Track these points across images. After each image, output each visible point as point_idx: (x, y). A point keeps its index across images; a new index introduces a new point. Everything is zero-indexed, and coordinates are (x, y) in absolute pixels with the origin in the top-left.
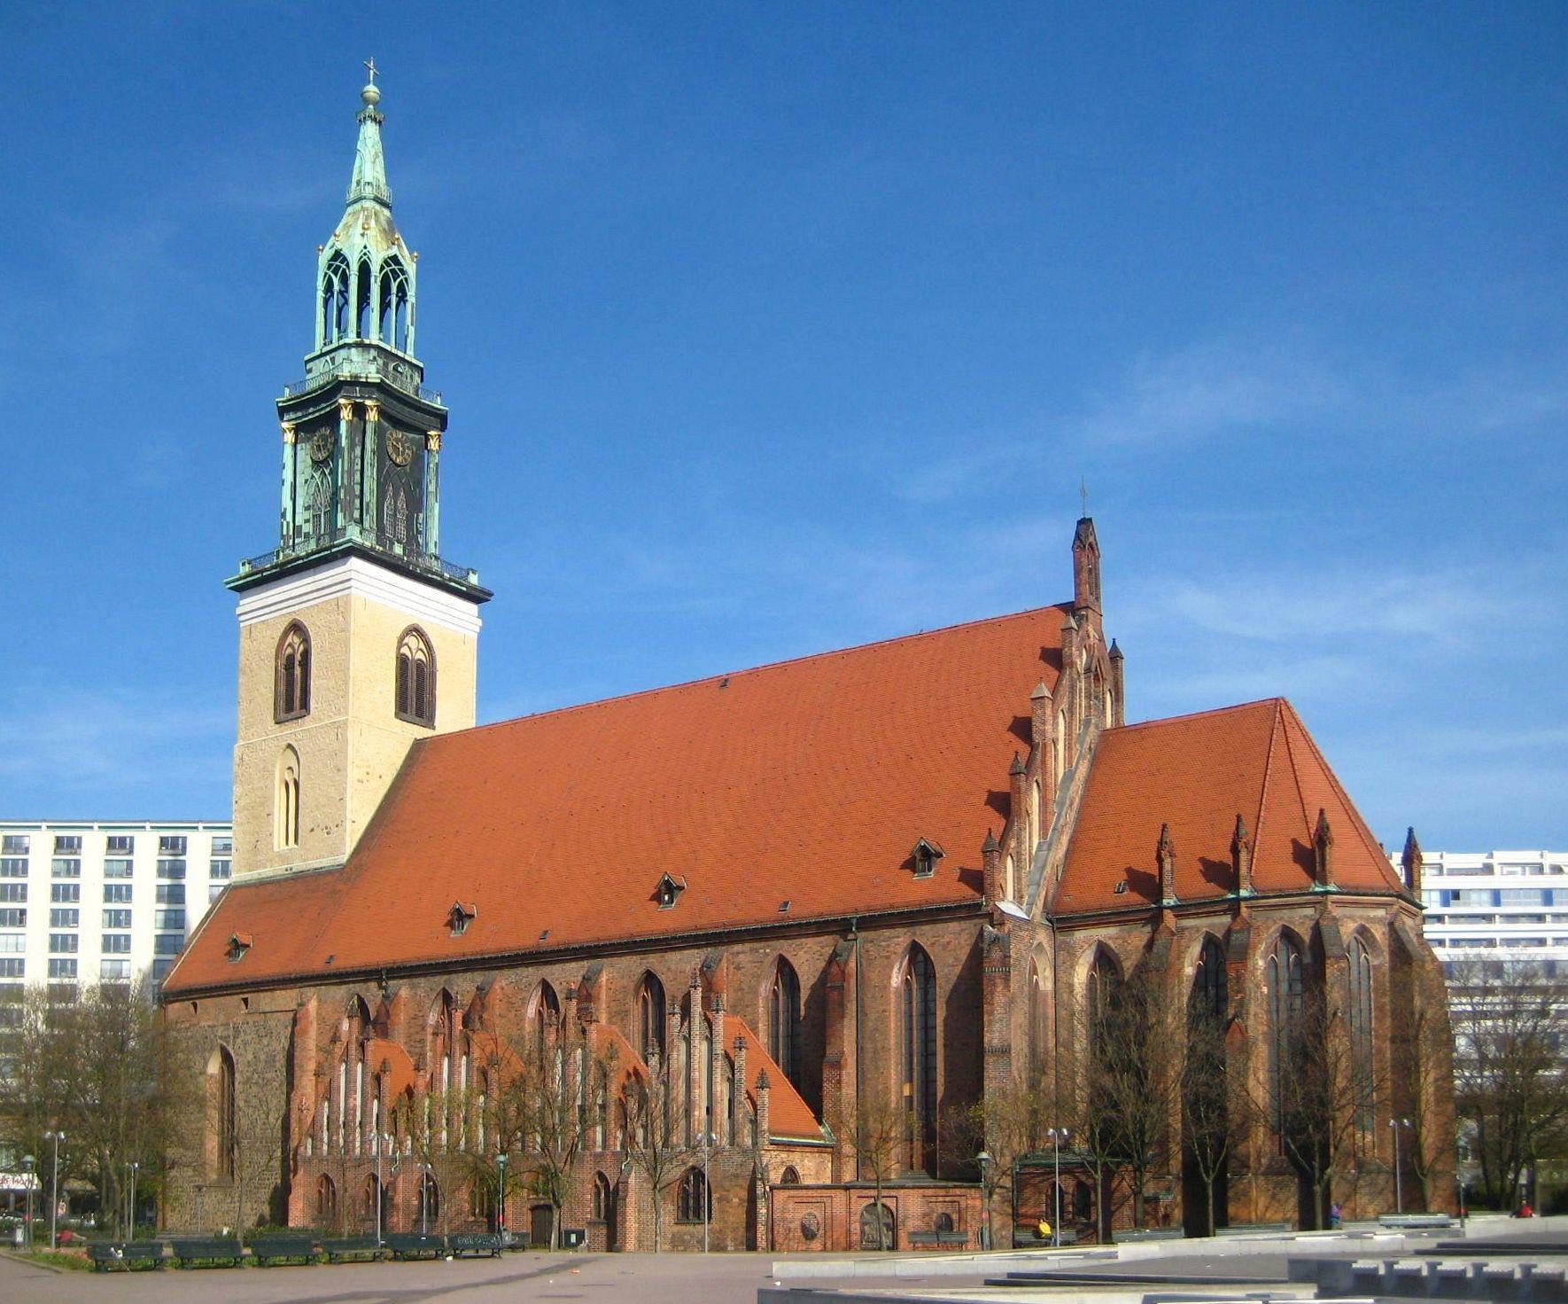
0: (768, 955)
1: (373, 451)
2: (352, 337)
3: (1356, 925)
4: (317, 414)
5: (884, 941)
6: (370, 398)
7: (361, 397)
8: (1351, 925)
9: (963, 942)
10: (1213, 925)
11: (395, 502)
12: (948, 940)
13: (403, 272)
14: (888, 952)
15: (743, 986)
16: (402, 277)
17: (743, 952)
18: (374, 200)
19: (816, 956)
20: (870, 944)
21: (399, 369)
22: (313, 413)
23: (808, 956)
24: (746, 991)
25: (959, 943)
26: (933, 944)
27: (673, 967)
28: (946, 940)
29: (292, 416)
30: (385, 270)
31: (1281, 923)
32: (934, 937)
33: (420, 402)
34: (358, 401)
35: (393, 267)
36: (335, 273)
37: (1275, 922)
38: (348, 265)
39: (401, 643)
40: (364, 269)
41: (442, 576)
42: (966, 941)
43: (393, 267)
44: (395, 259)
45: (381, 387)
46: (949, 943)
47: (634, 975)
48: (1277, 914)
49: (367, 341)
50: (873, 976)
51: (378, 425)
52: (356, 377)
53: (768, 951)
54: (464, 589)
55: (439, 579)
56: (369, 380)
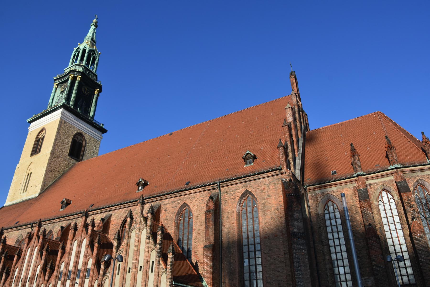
0: (179, 203)
2: (77, 63)
5: (232, 192)
6: (79, 75)
9: (271, 188)
10: (384, 181)
12: (263, 188)
14: (234, 196)
15: (168, 218)
17: (169, 203)
19: (201, 202)
20: (226, 194)
22: (63, 80)
23: (197, 202)
24: (169, 220)
25: (269, 189)
26: (256, 190)
28: (263, 187)
29: (57, 81)
32: (256, 187)
34: (75, 75)
36: (77, 52)
37: (415, 178)
38: (80, 50)
39: (75, 136)
40: (84, 51)
42: (272, 187)
46: (264, 189)
48: (415, 174)
49: (81, 64)
50: (227, 208)
52: (76, 70)
53: (179, 202)
54: (98, 127)
56: (79, 71)
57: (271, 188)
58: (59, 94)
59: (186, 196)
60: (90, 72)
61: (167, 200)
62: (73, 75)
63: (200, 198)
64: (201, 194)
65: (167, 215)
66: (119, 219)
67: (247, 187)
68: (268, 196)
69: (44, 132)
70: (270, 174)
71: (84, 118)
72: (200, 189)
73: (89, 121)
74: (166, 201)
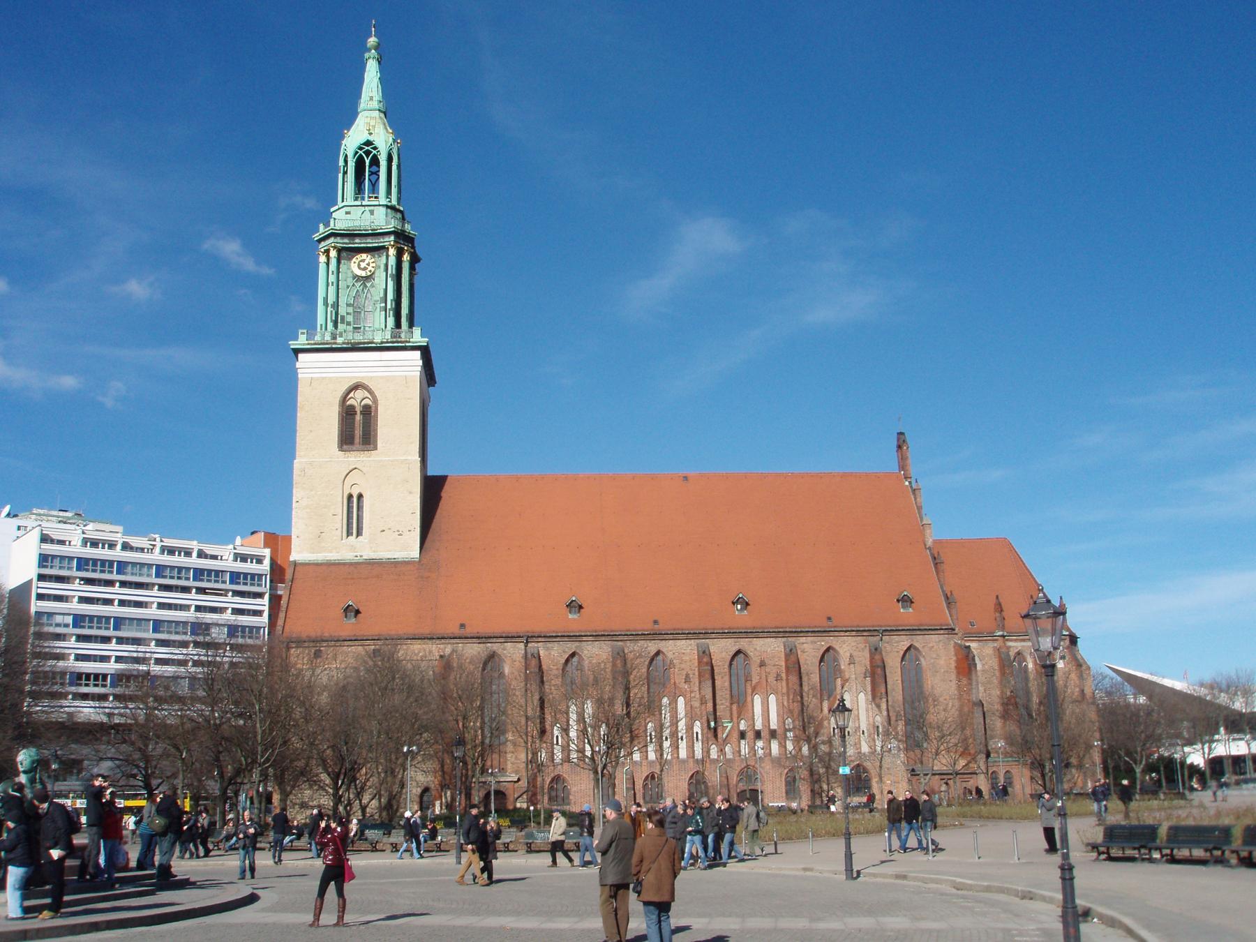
0: (823, 645)
4: (362, 245)
9: (941, 647)
15: (807, 662)
19: (854, 648)
23: (848, 648)
26: (924, 647)
27: (758, 648)
28: (931, 645)
34: (402, 246)
46: (933, 647)
47: (730, 652)
53: (823, 643)
56: (410, 235)
57: (941, 647)
58: (350, 281)
59: (831, 638)
61: (804, 638)
63: (854, 644)
64: (854, 639)
65: (807, 658)
66: (724, 653)
67: (913, 640)
68: (938, 655)
69: (359, 394)
70: (942, 632)
72: (854, 633)
74: (803, 640)
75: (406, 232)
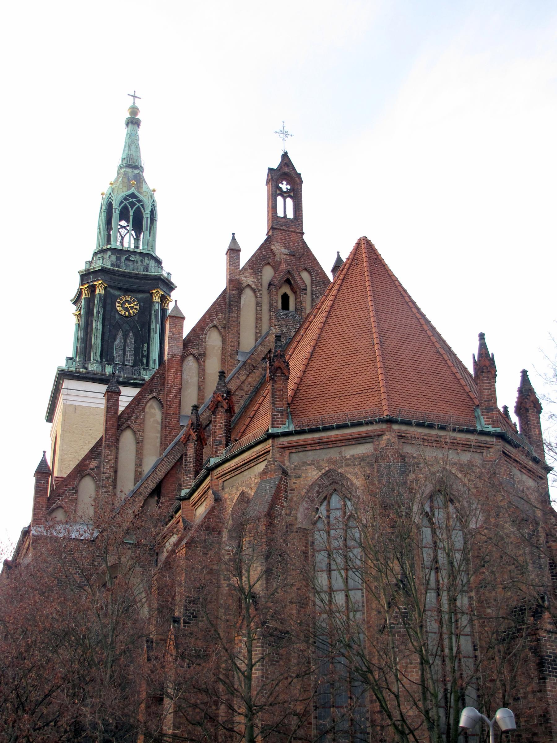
1: (98, 312)
3: (320, 474)
6: (98, 280)
7: (94, 281)
8: (315, 473)
11: (125, 342)
13: (139, 201)
16: (138, 204)
18: (126, 167)
21: (131, 259)
30: (123, 205)
31: (241, 489)
33: (140, 274)
34: (91, 284)
35: (131, 200)
41: (143, 380)
43: (134, 200)
44: (133, 195)
45: (103, 270)
51: (105, 299)
55: (141, 382)
56: (95, 269)
60: (130, 256)
62: (87, 286)
71: (121, 380)
73: (137, 381)
75: (90, 269)
